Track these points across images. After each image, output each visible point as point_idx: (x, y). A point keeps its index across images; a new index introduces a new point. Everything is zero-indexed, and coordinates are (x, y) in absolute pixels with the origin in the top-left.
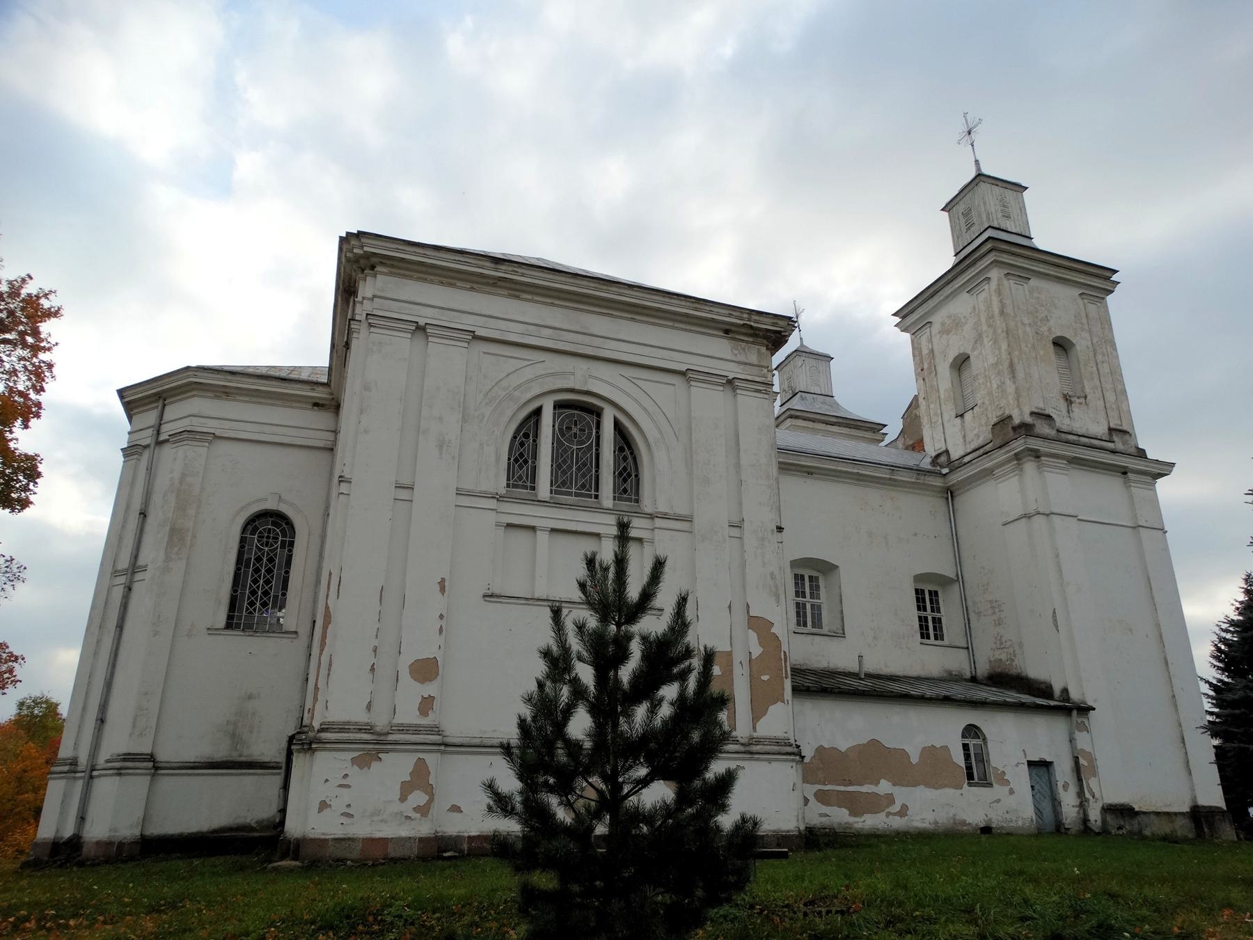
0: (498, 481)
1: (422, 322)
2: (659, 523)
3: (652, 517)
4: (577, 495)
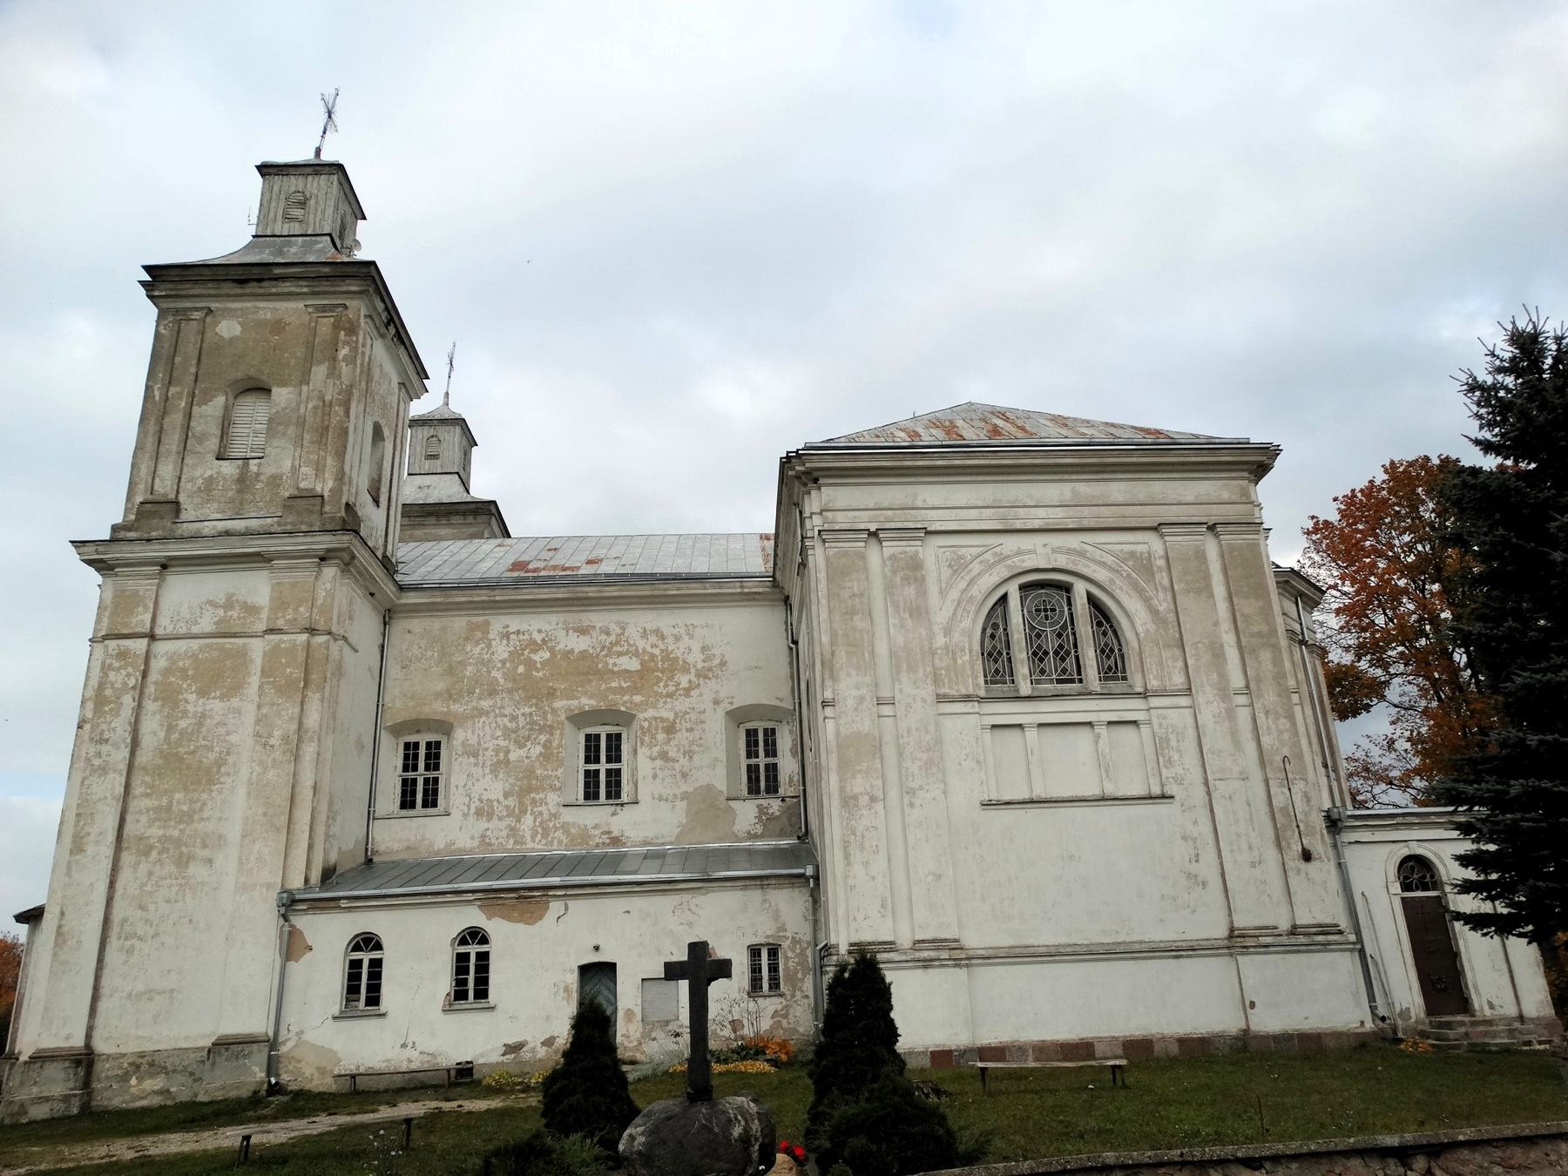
0: (975, 682)
1: (873, 529)
2: (1154, 702)
3: (1144, 695)
4: (1059, 681)
